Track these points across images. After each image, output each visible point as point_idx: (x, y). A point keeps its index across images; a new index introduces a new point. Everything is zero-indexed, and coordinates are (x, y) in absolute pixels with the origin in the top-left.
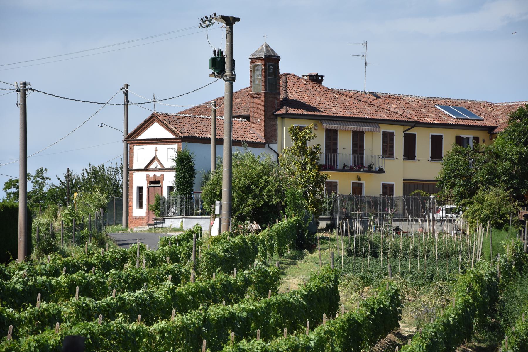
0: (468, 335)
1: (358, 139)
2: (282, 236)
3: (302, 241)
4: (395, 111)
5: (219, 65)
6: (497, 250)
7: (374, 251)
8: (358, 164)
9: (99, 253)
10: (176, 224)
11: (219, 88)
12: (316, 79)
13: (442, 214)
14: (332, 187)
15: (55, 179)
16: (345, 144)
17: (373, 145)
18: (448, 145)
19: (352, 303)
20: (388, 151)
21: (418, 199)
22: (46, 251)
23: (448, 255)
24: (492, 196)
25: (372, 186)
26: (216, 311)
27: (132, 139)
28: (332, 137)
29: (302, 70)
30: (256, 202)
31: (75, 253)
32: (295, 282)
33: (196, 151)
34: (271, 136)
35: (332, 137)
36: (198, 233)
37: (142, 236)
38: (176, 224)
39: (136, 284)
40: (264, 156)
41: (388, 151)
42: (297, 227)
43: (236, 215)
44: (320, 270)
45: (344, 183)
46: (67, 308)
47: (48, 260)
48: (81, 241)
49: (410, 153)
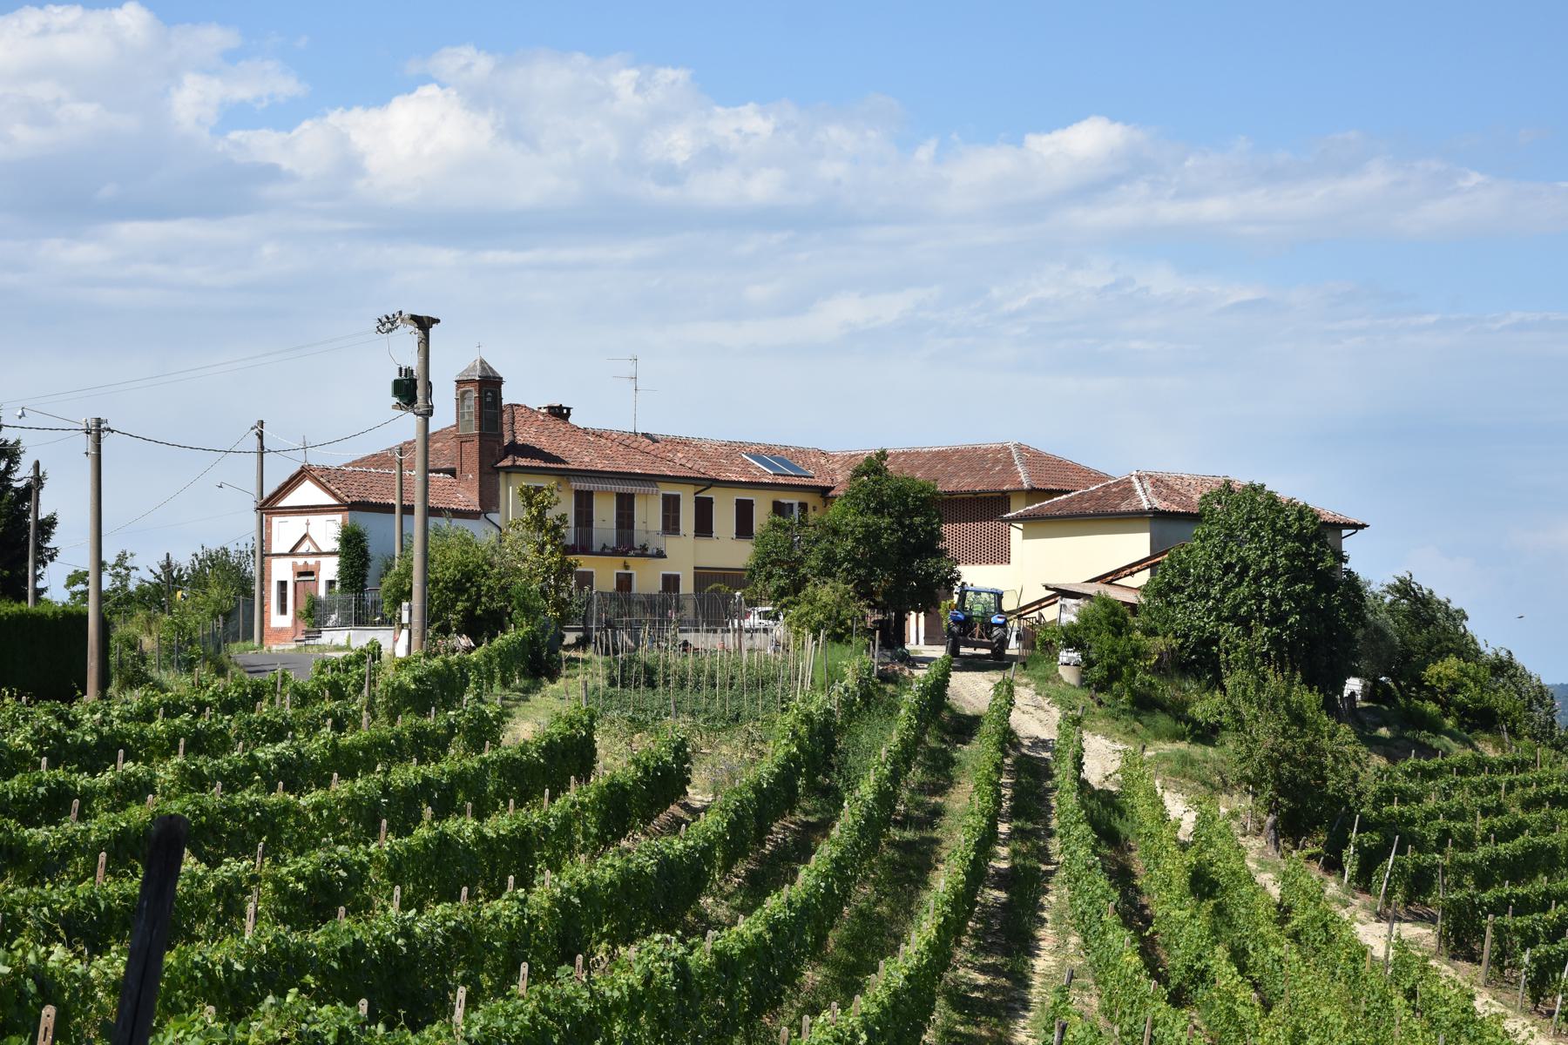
0: (790, 803)
1: (625, 506)
2: (507, 658)
3: (539, 665)
4: (681, 463)
5: (408, 390)
6: (834, 675)
7: (650, 677)
8: (626, 545)
10: (340, 639)
11: (407, 426)
13: (753, 621)
14: (586, 579)
15: (145, 571)
16: (605, 514)
17: (648, 515)
18: (762, 516)
19: (615, 758)
20: (671, 525)
21: (717, 597)
23: (761, 683)
24: (827, 593)
25: (647, 578)
27: (269, 506)
28: (584, 502)
30: (465, 602)
31: (178, 684)
32: (529, 725)
33: (370, 524)
34: (489, 500)
35: (584, 502)
36: (375, 652)
37: (284, 658)
38: (340, 639)
39: (276, 733)
40: (481, 533)
41: (671, 525)
42: (531, 643)
43: (436, 622)
44: (566, 708)
45: (604, 573)
46: (166, 772)
47: (136, 697)
48: (190, 665)
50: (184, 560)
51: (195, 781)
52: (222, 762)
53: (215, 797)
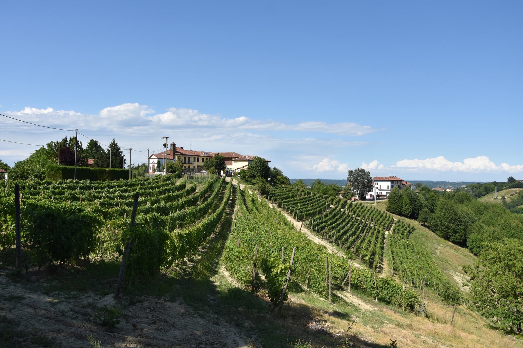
0: (208, 192)
1: (189, 158)
2: (176, 175)
3: (179, 176)
4: (196, 154)
5: (165, 145)
6: (213, 178)
7: (192, 178)
8: (189, 163)
9: (145, 178)
10: (157, 173)
11: (165, 149)
12: (182, 148)
13: (204, 171)
14: (185, 167)
15: (136, 165)
16: (187, 159)
17: (192, 159)
18: (205, 160)
19: (188, 187)
20: (194, 161)
21: (200, 169)
22: (134, 178)
23: (204, 178)
24: (212, 168)
25: (192, 167)
26: (164, 188)
27: (149, 158)
28: (185, 158)
29: (180, 147)
30: (171, 169)
31: (139, 178)
32: (178, 183)
33: (160, 160)
34: (174, 158)
35: (185, 158)
36: (161, 175)
37: (151, 175)
38: (157, 173)
39: (150, 183)
40: (173, 161)
41: (194, 161)
42: (179, 174)
43: (168, 171)
44: (183, 181)
45: (187, 166)
46: (138, 187)
47: (135, 179)
48: (140, 176)
49: (198, 161)
50: (140, 164)
51: (141, 189)
52: (144, 187)
53: (143, 191)
